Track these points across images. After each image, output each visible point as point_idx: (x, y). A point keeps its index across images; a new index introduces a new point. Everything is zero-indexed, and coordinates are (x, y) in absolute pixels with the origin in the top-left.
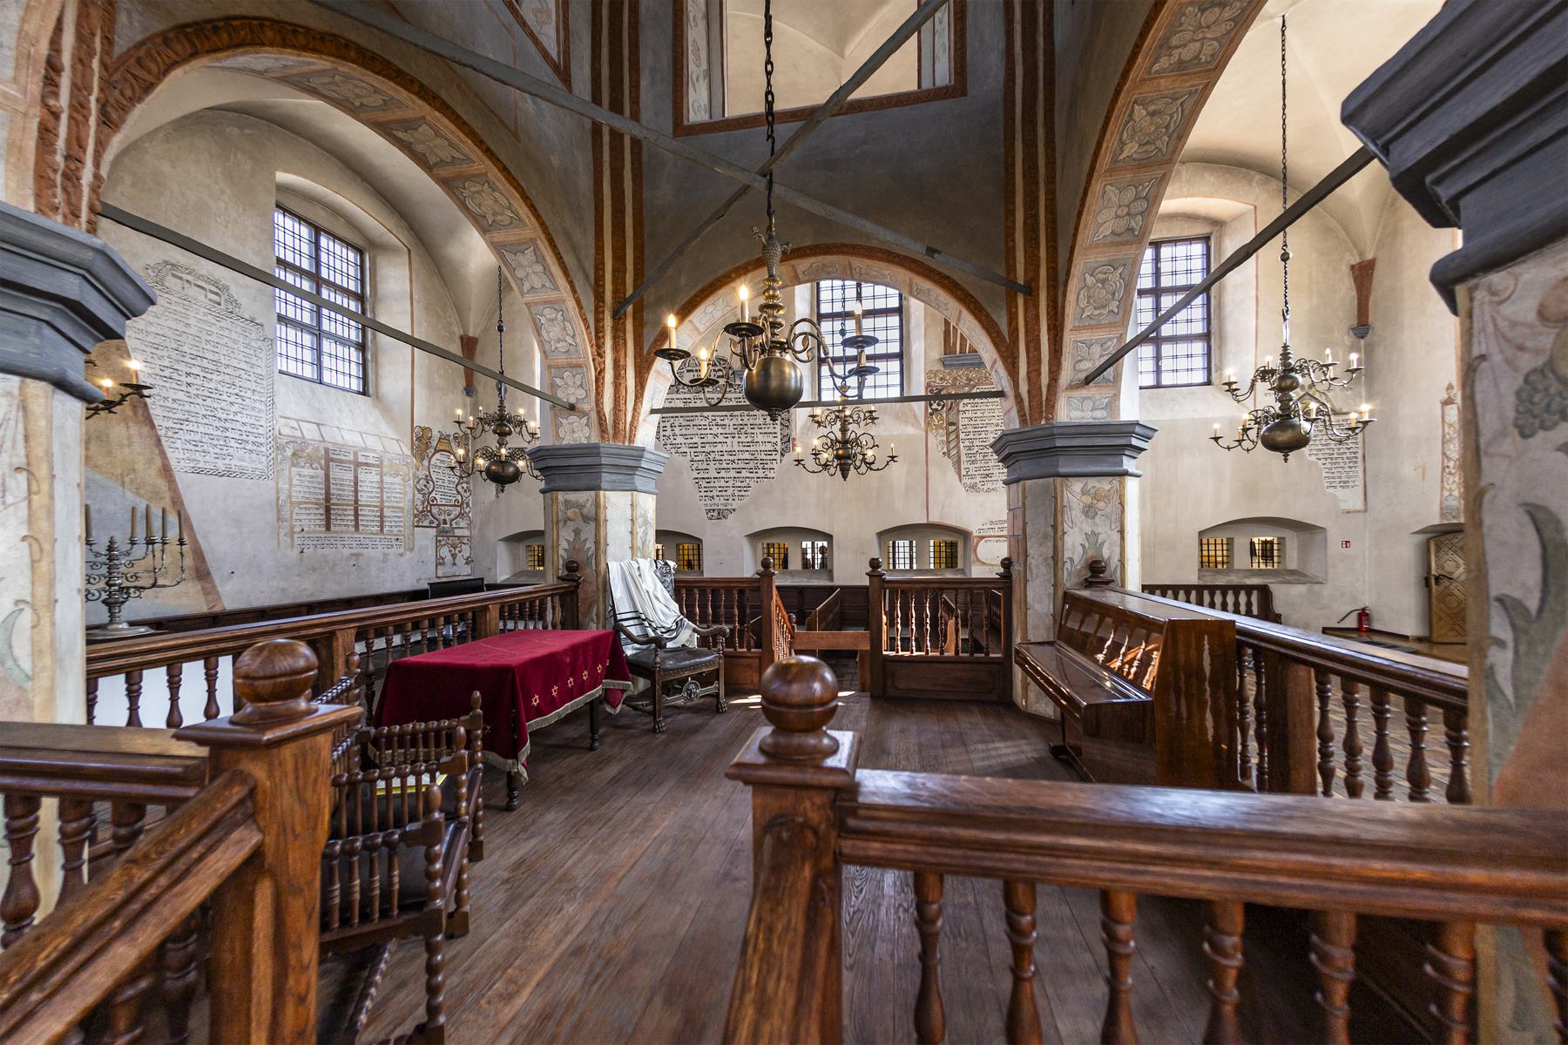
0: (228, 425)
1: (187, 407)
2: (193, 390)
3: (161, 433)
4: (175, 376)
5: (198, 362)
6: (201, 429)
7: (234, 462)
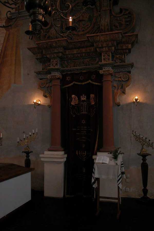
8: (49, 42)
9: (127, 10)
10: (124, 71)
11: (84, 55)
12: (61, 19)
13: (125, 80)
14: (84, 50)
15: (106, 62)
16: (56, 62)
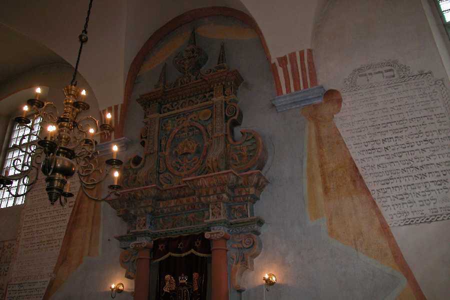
0: (424, 171)
1: (389, 168)
2: (390, 152)
3: (375, 196)
4: (376, 146)
5: (390, 127)
6: (404, 183)
7: (438, 205)
8: (131, 191)
9: (251, 134)
13: (248, 246)
15: (215, 219)
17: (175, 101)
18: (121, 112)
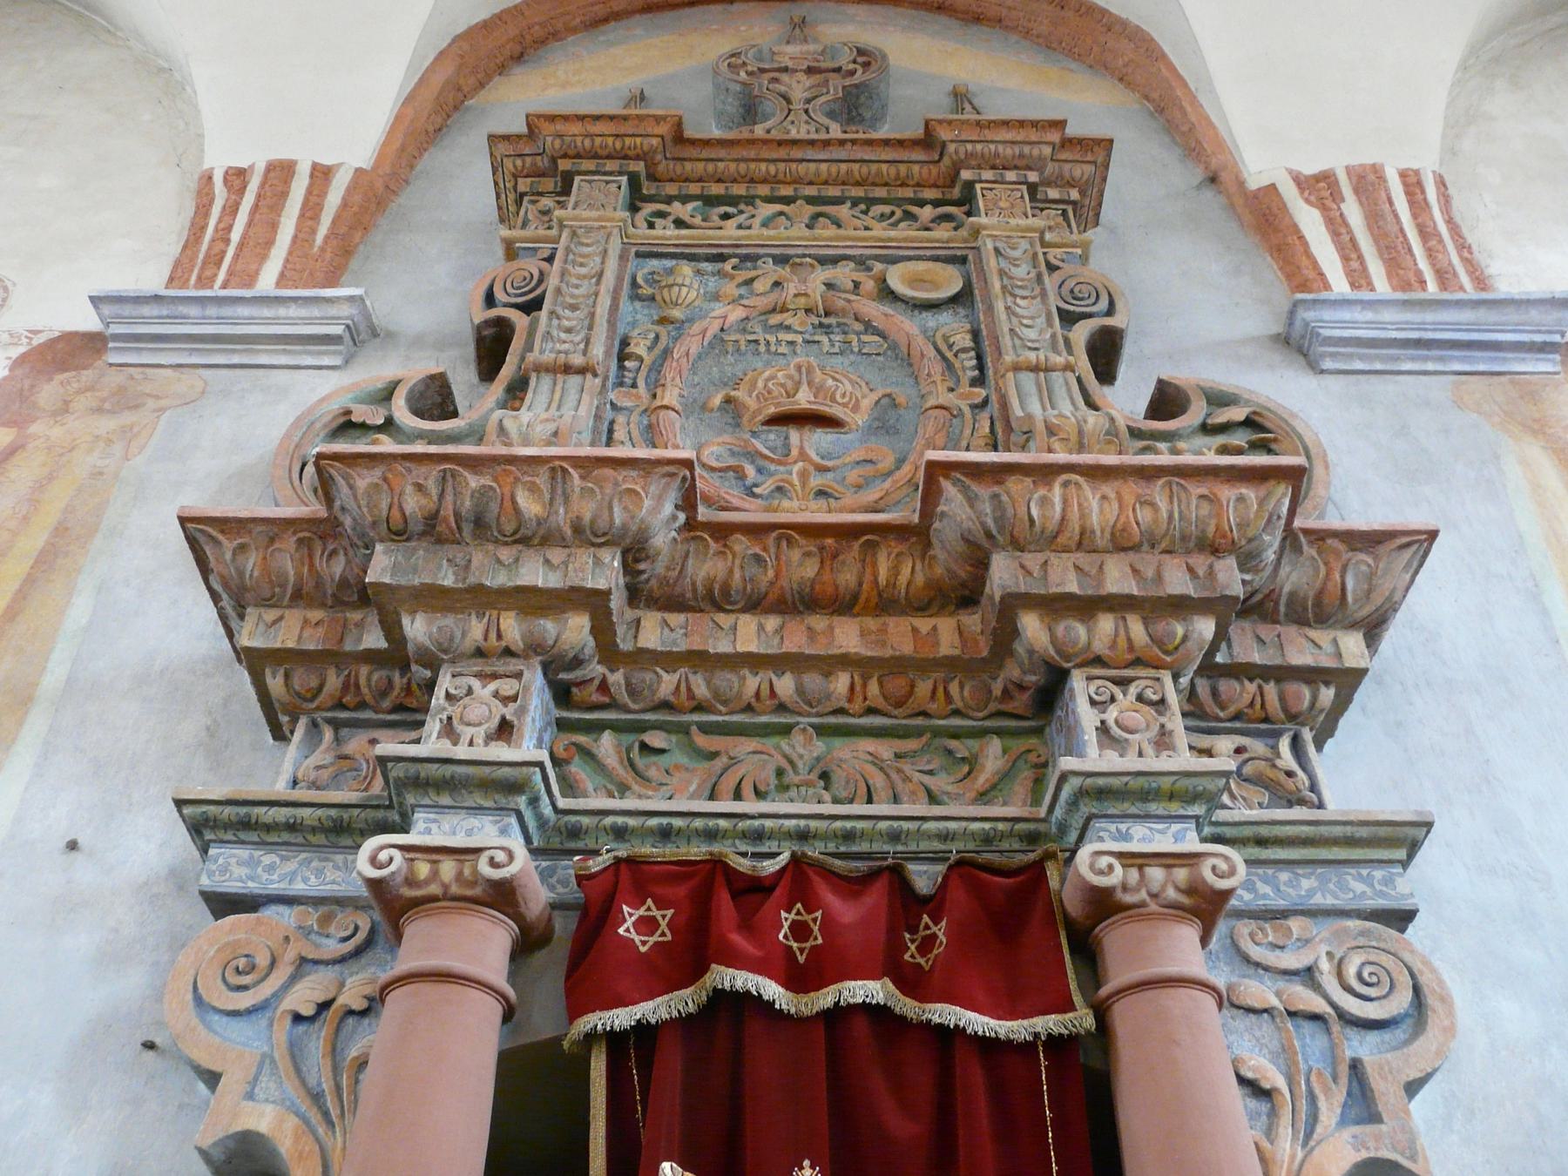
10: (1329, 901)
11: (841, 683)
12: (604, 385)
14: (848, 636)
16: (499, 710)
17: (733, 201)
18: (345, 204)
